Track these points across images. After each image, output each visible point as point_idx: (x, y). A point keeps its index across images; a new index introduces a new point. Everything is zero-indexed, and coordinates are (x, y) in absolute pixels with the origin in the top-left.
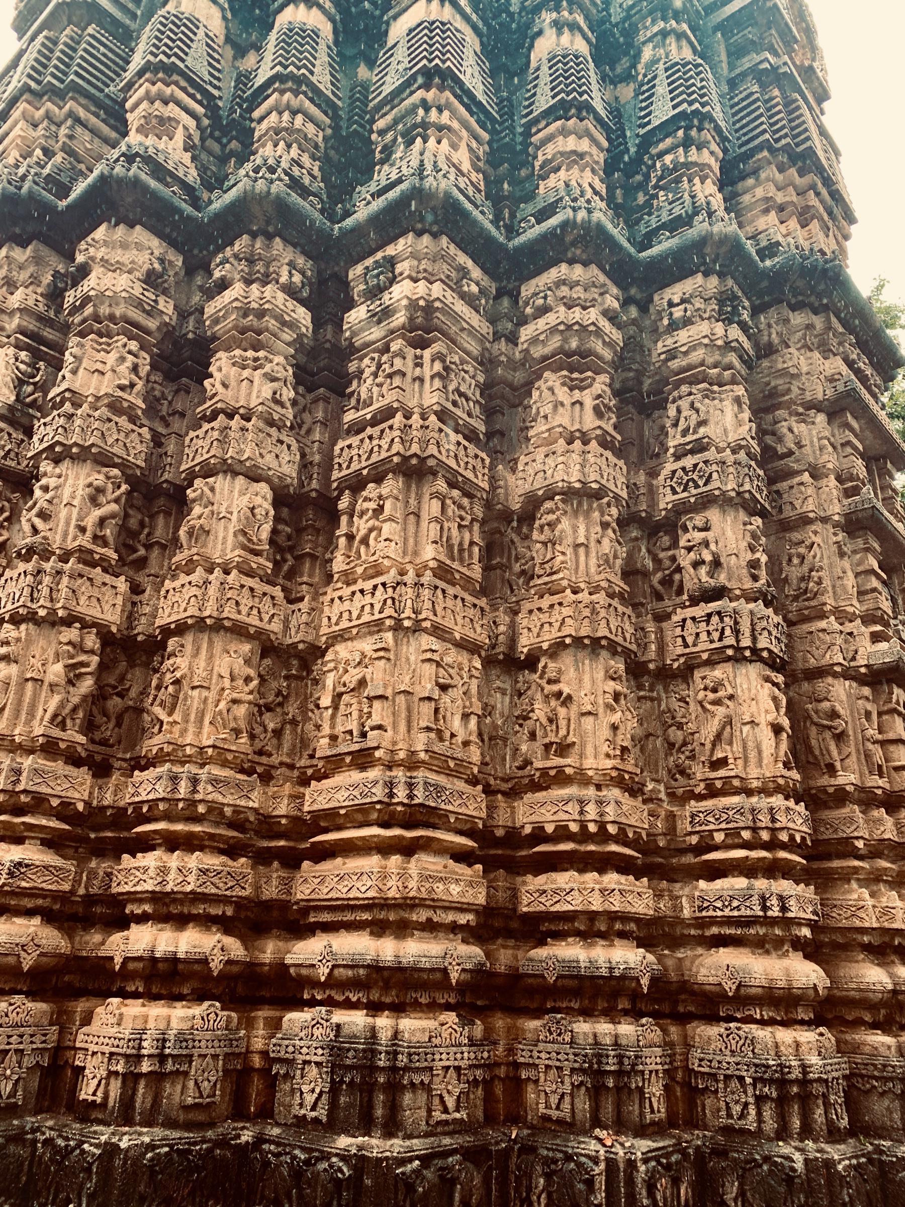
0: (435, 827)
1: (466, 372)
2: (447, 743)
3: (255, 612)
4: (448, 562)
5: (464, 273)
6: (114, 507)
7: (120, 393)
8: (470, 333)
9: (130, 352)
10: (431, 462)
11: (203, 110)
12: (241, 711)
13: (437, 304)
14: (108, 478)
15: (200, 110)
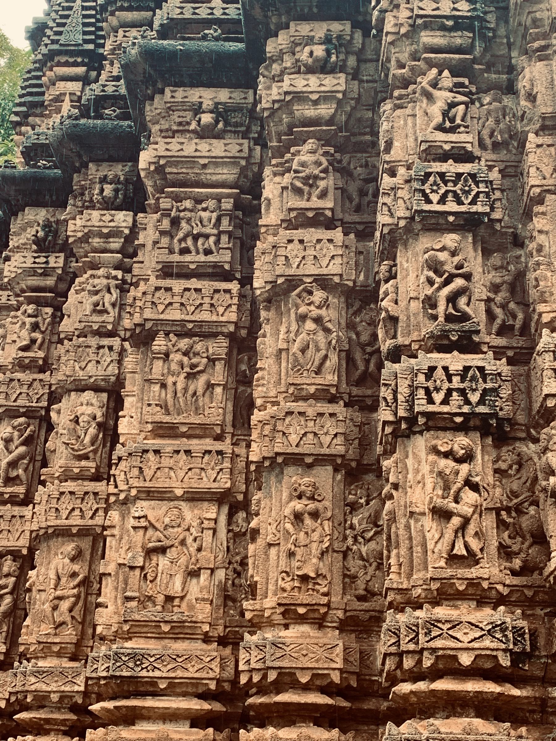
0: (155, 694)
1: (204, 210)
2: (159, 608)
3: (77, 512)
4: (167, 419)
5: (197, 109)
6: (22, 449)
7: (21, 354)
8: (216, 164)
9: (29, 316)
10: (148, 325)
11: (84, 69)
12: (65, 605)
13: (162, 162)
14: (14, 428)
15: (80, 70)
